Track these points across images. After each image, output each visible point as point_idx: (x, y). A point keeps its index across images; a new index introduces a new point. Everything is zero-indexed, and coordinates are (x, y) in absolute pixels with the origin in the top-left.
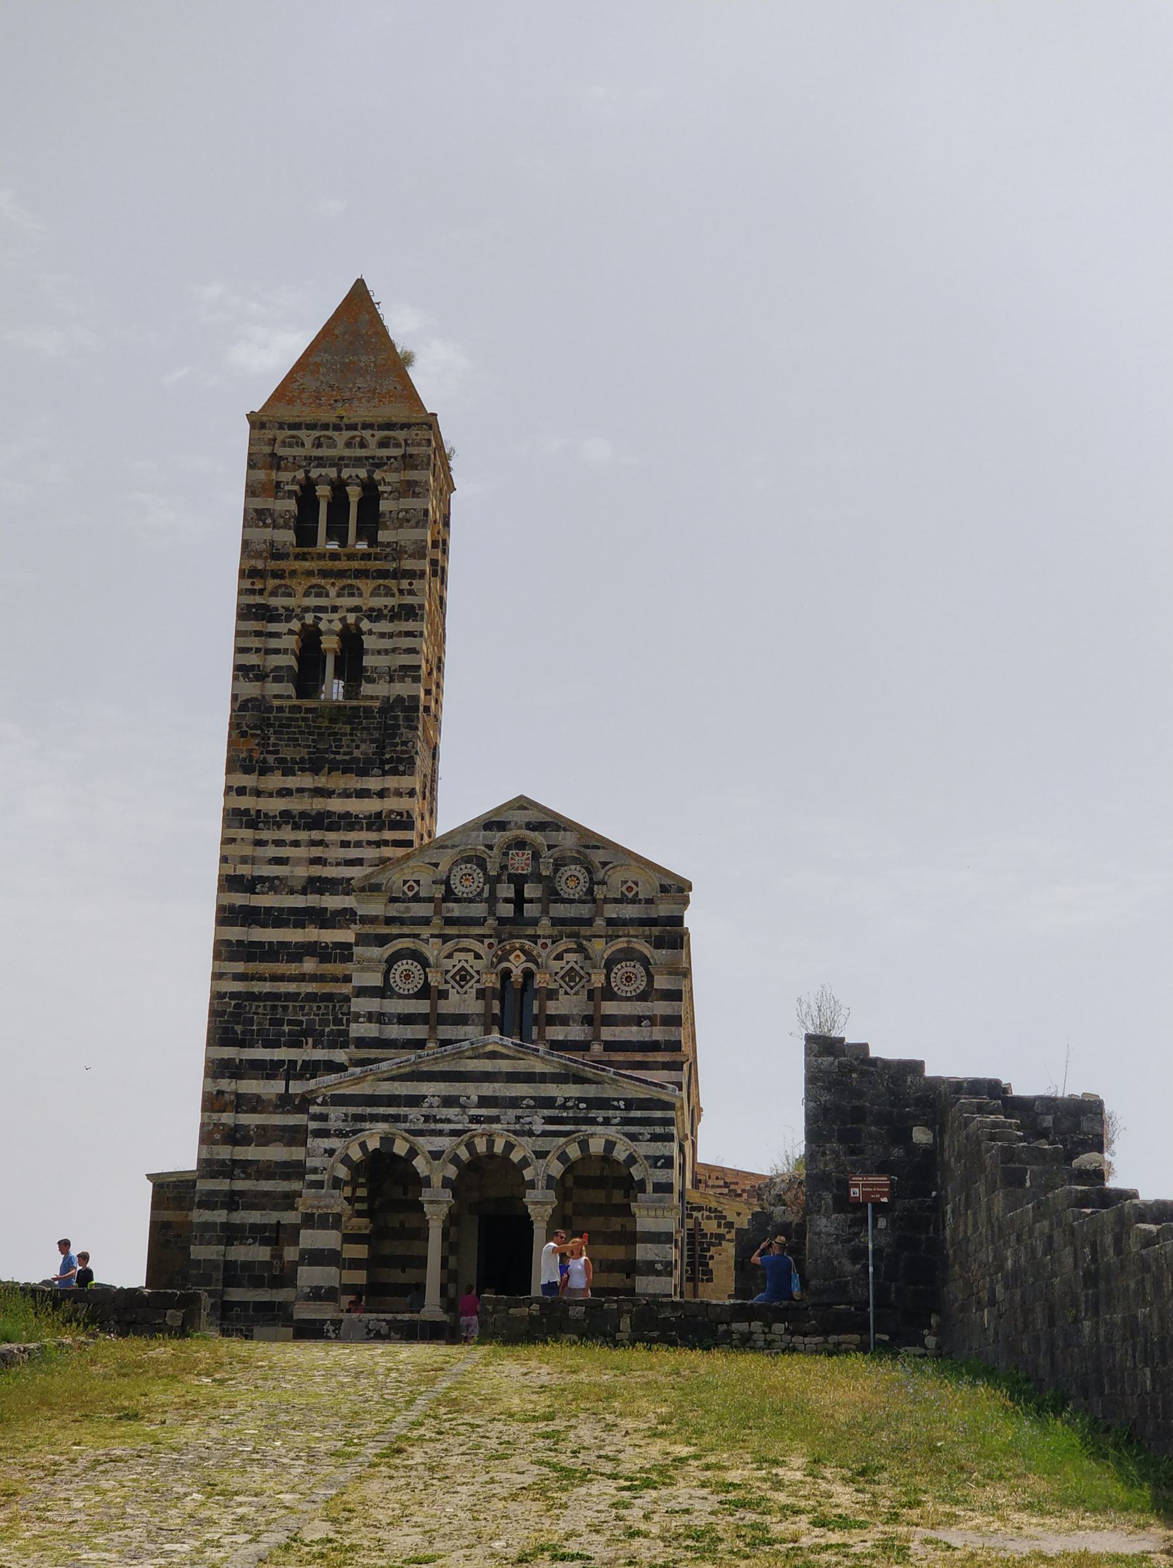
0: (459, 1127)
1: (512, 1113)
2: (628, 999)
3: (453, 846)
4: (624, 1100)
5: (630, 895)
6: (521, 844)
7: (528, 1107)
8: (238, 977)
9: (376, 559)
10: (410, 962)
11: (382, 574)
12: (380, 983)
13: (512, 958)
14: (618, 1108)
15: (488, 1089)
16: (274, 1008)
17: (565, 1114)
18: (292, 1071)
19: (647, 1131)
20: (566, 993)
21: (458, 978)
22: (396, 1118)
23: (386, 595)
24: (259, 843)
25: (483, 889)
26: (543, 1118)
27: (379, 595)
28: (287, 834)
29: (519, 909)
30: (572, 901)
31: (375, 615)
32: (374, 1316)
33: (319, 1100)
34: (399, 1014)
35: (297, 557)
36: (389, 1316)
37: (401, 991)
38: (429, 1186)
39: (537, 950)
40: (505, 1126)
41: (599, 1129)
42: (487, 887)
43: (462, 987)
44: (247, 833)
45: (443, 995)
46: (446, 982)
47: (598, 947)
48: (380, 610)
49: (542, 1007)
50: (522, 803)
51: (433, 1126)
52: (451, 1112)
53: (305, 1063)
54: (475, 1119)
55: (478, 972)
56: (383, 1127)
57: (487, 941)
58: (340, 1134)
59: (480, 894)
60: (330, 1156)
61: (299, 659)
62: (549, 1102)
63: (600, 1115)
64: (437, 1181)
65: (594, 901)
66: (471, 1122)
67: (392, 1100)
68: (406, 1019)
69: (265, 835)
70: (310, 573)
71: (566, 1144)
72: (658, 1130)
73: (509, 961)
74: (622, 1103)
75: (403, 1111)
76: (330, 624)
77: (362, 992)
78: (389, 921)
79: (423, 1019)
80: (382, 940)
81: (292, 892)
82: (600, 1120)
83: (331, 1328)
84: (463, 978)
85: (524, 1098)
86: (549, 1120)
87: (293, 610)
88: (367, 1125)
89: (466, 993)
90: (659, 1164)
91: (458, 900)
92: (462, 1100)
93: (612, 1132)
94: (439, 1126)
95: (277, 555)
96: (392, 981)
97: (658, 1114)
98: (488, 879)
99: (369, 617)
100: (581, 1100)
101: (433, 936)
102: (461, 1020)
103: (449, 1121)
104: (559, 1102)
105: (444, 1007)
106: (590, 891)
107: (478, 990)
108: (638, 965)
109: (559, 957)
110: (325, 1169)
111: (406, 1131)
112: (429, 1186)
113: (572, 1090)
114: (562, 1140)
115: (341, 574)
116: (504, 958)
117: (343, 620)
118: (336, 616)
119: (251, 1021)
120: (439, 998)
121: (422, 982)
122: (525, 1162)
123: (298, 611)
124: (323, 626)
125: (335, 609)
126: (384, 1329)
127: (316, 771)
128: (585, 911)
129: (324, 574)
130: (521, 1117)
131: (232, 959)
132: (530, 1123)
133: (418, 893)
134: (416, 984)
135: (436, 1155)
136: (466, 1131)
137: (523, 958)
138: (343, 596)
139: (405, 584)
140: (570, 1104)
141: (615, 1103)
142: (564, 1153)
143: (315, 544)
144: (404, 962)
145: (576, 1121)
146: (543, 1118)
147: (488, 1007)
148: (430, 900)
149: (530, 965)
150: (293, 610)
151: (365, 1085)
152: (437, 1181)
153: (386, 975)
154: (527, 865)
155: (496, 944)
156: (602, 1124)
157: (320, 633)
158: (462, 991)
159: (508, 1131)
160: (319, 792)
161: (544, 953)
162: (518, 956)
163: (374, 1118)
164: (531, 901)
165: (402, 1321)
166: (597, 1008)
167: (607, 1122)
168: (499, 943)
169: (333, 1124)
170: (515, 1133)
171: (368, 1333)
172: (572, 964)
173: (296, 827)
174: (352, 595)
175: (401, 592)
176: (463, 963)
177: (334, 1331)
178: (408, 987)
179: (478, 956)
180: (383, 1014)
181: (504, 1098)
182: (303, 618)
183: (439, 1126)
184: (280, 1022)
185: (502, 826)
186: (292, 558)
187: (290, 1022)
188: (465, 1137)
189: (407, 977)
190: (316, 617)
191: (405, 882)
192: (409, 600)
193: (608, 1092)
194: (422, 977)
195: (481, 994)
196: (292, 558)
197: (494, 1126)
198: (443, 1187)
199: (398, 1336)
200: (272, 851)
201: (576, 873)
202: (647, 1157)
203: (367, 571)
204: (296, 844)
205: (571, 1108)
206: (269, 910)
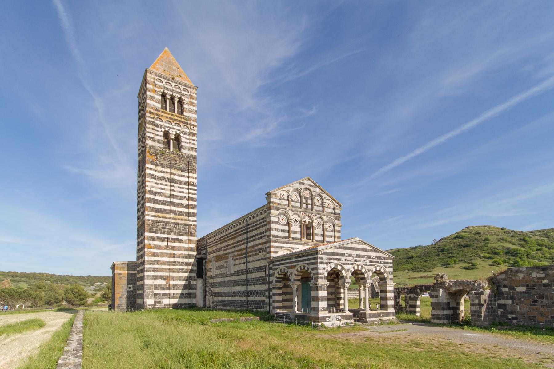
8: (153, 216)
16: (163, 225)
18: (168, 240)
24: (156, 183)
28: (163, 182)
44: (153, 180)
52: (350, 258)
53: (172, 239)
68: (283, 231)
69: (158, 182)
81: (166, 197)
102: (295, 232)
103: (350, 261)
119: (157, 227)
127: (171, 168)
131: (151, 211)
135: (348, 270)
160: (171, 173)
173: (166, 181)
184: (164, 228)
187: (167, 229)
200: (160, 186)
204: (166, 185)
206: (160, 201)
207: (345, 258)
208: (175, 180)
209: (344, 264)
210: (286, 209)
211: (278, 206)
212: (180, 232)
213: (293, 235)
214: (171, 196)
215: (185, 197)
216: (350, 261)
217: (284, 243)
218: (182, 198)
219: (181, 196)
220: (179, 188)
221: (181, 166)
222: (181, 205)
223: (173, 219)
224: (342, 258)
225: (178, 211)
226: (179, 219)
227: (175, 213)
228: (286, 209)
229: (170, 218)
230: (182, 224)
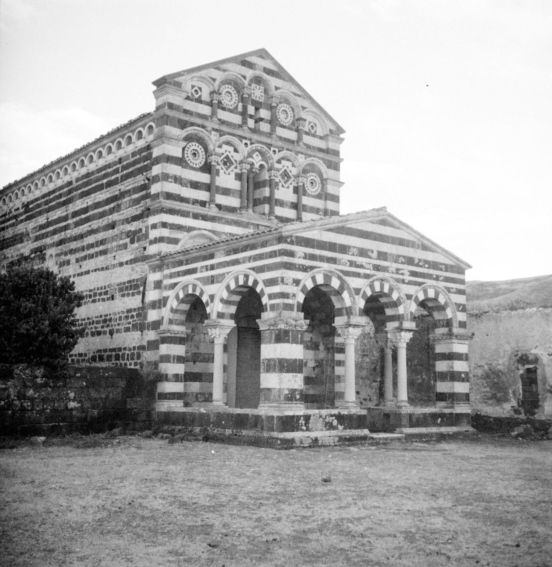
0: (368, 272)
2: (313, 196)
3: (224, 71)
4: (445, 265)
5: (313, 131)
6: (258, 80)
12: (180, 155)
13: (254, 156)
20: (283, 186)
25: (237, 106)
30: (284, 127)
33: (289, 240)
37: (191, 164)
41: (434, 283)
42: (240, 105)
49: (272, 192)
50: (263, 54)
54: (377, 268)
55: (236, 161)
56: (326, 266)
57: (244, 141)
62: (410, 261)
65: (297, 130)
67: (332, 247)
68: (195, 185)
73: (252, 157)
74: (443, 267)
78: (186, 112)
80: (183, 125)
82: (434, 276)
86: (413, 274)
90: (460, 309)
98: (242, 99)
102: (226, 192)
103: (361, 266)
106: (293, 123)
107: (236, 174)
108: (317, 177)
109: (279, 162)
116: (250, 155)
121: (204, 160)
126: (335, 423)
128: (292, 135)
133: (200, 97)
134: (200, 161)
135: (357, 291)
137: (260, 158)
140: (421, 264)
141: (441, 266)
146: (409, 271)
147: (242, 186)
148: (210, 104)
149: (263, 163)
153: (184, 149)
154: (262, 96)
162: (257, 155)
163: (322, 259)
164: (261, 119)
166: (299, 199)
167: (437, 278)
169: (298, 261)
172: (285, 168)
179: (236, 151)
185: (250, 65)
189: (194, 154)
191: (193, 87)
195: (239, 177)
197: (386, 275)
201: (287, 110)
202: (456, 304)
209: (347, 274)
213: (220, 199)
216: (361, 266)
217: (196, 216)
224: (345, 257)
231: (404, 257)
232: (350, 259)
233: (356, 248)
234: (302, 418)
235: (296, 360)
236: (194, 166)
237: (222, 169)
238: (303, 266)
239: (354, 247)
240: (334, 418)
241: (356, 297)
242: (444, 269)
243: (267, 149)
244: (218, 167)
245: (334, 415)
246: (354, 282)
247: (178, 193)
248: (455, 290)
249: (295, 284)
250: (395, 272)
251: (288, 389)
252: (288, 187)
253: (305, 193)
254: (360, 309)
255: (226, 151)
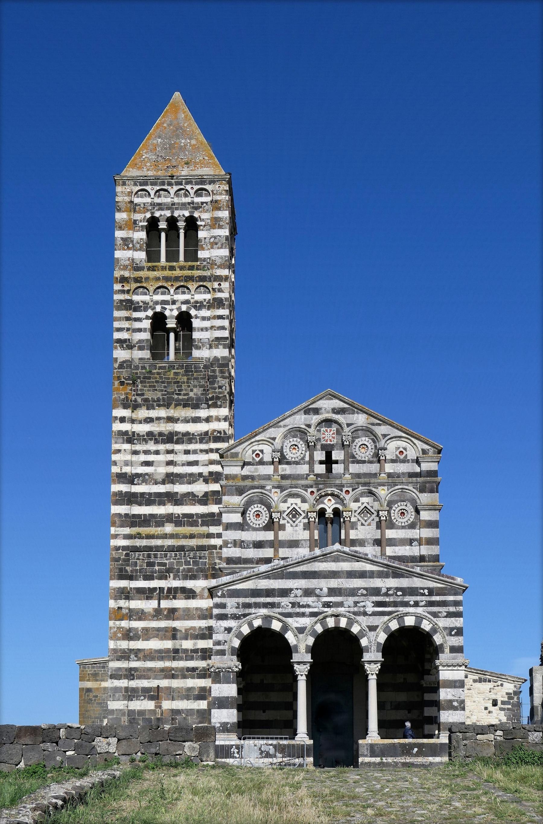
0: (316, 610)
1: (350, 600)
4: (428, 589)
7: (363, 595)
9: (197, 269)
10: (259, 505)
11: (202, 279)
14: (423, 595)
15: (334, 583)
17: (387, 600)
19: (443, 610)
21: (291, 516)
22: (272, 605)
23: (205, 293)
26: (373, 602)
27: (201, 293)
29: (329, 470)
31: (199, 306)
32: (265, 742)
33: (219, 594)
34: (254, 541)
35: (149, 269)
36: (275, 742)
37: (254, 526)
38: (297, 652)
39: (343, 495)
40: (347, 609)
41: (411, 610)
43: (294, 522)
45: (282, 527)
46: (284, 519)
47: (382, 492)
48: (201, 302)
51: (298, 610)
52: (309, 600)
54: (327, 605)
55: (304, 511)
56: (264, 611)
58: (235, 617)
59: (303, 458)
60: (229, 632)
61: (152, 335)
62: (376, 591)
63: (411, 599)
64: (302, 648)
66: (324, 606)
67: (269, 593)
68: (259, 545)
70: (157, 279)
71: (390, 620)
72: (452, 609)
73: (325, 504)
74: (426, 591)
75: (276, 600)
76: (171, 312)
77: (229, 527)
79: (271, 544)
82: (412, 603)
83: (236, 751)
84: (294, 516)
85: (359, 589)
86: (378, 604)
87: (148, 304)
88: (253, 610)
89: (296, 526)
91: (288, 463)
92: (317, 592)
93: (419, 610)
94: (302, 610)
95: (138, 268)
96: (248, 518)
97: (451, 598)
99: (195, 307)
100: (398, 589)
101: (274, 487)
103: (308, 606)
104: (384, 590)
105: (283, 536)
110: (226, 642)
111: (280, 614)
112: (297, 652)
113: (392, 583)
114: (386, 618)
115: (177, 279)
117: (179, 309)
118: (174, 307)
120: (280, 530)
121: (267, 519)
122: (362, 633)
123: (151, 304)
124: (167, 313)
125: (174, 302)
126: (272, 751)
129: (167, 279)
130: (358, 602)
132: (364, 606)
135: (301, 630)
136: (321, 613)
137: (333, 501)
138: (178, 293)
139: (216, 285)
140: (391, 592)
141: (422, 591)
142: (388, 627)
143: (159, 261)
144: (256, 506)
145: (395, 604)
146: (373, 602)
150: (148, 304)
151: (250, 582)
152: (302, 648)
155: (315, 491)
156: (413, 606)
157: (165, 317)
158: (294, 525)
159: (349, 612)
161: (347, 497)
163: (257, 605)
165: (284, 745)
167: (416, 604)
168: (318, 491)
169: (229, 610)
170: (355, 613)
171: (261, 754)
174: (184, 293)
175: (214, 290)
176: (294, 506)
177: (238, 753)
178: (258, 522)
180: (243, 541)
181: (346, 589)
182: (155, 308)
183: (302, 610)
186: (146, 270)
188: (320, 617)
190: (162, 307)
192: (219, 295)
193: (417, 582)
194: (268, 515)
195: (307, 526)
196: (146, 270)
197: (341, 610)
198: (306, 652)
199: (281, 755)
202: (445, 628)
203: (193, 277)
205: (392, 595)
207: (292, 599)
208: (177, 433)
209: (289, 615)
210: (263, 487)
211: (241, 483)
212: (189, 570)
213: (283, 552)
214: (170, 478)
215: (200, 475)
216: (308, 606)
218: (192, 478)
219: (191, 475)
220: (187, 452)
221: (191, 394)
222: (191, 498)
223: (172, 536)
225: (185, 515)
226: (185, 537)
227: (177, 520)
228: (263, 487)
229: (165, 536)
230: (192, 549)
231: (364, 589)
232: (292, 601)
233: (301, 589)
234: (234, 747)
235: (228, 697)
236: (257, 526)
237: (288, 522)
238: (235, 615)
239: (297, 589)
240: (271, 747)
241: (301, 636)
242: (427, 594)
243: (339, 491)
244: (282, 522)
245: (271, 745)
246: (294, 622)
247: (238, 556)
248: (445, 614)
249: (226, 632)
250: (352, 605)
251: (220, 723)
252: (369, 525)
253: (391, 525)
254: (379, 644)
255: (292, 504)
